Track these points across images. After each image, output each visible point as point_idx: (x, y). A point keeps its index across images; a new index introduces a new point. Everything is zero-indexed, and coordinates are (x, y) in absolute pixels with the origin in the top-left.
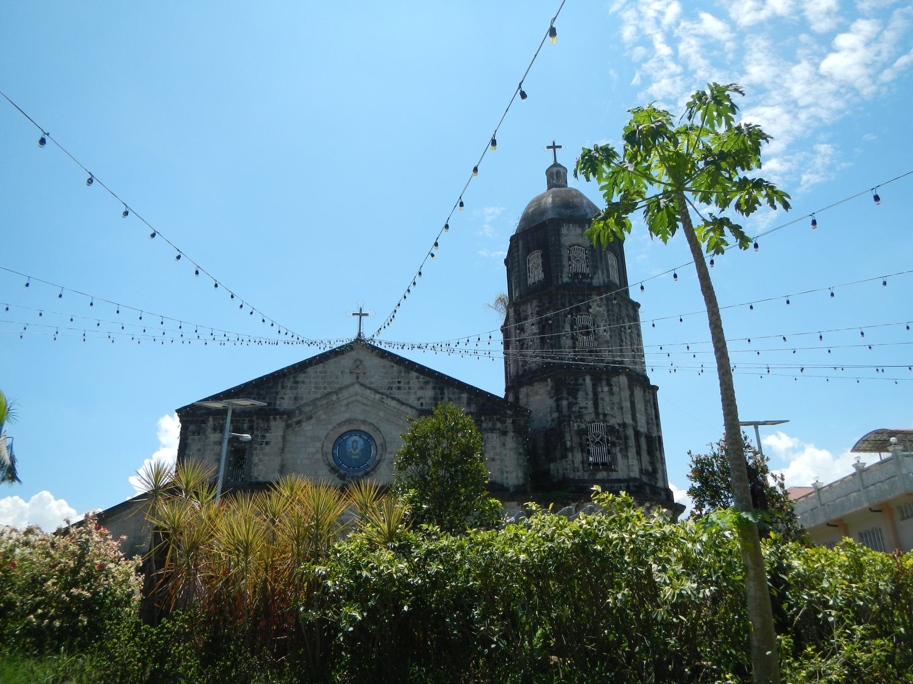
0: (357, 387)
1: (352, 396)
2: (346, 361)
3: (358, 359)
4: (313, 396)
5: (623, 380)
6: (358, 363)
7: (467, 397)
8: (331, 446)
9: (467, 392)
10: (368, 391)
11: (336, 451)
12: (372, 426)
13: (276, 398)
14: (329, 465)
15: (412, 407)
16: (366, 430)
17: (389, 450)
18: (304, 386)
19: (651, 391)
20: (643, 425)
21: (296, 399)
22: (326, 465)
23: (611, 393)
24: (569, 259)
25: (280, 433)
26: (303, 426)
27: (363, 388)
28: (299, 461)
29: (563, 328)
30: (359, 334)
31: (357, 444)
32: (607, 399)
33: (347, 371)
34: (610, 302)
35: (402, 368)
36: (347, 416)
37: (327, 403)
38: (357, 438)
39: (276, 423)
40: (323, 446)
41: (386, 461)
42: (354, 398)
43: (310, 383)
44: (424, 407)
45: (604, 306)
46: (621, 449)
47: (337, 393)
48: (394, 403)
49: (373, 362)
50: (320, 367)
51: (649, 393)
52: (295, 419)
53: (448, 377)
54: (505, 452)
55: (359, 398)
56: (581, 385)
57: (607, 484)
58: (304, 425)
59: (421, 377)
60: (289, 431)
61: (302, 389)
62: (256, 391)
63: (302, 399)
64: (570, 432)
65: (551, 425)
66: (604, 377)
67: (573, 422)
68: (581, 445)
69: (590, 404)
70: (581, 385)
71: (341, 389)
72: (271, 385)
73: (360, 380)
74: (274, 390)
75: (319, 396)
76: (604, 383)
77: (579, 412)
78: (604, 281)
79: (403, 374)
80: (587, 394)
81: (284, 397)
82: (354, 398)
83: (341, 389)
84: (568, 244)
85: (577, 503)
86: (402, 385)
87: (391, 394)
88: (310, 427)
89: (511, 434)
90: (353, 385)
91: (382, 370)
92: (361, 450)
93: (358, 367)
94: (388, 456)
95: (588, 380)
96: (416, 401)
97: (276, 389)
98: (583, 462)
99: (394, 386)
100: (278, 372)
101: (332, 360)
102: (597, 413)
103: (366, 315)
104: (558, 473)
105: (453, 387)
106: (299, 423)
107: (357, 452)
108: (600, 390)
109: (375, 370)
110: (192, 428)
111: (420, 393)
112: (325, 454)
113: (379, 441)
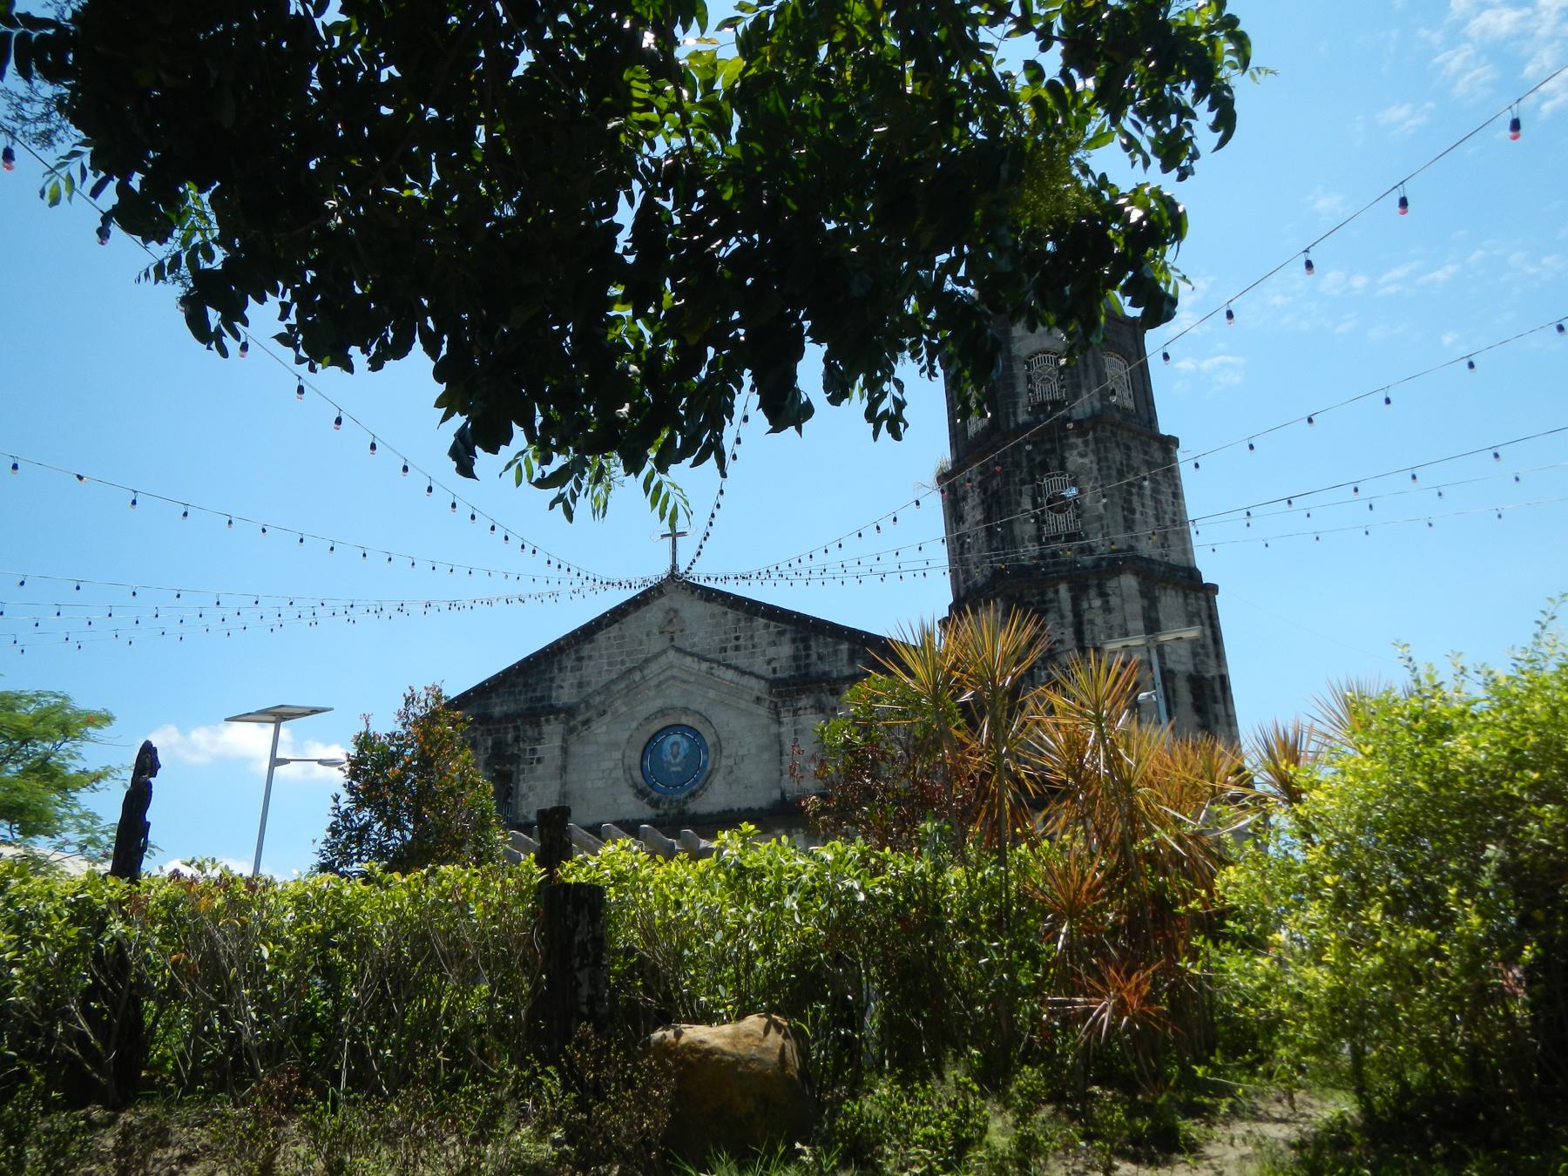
0: (672, 654)
1: (663, 671)
2: (653, 614)
3: (671, 609)
4: (605, 678)
5: (1129, 582)
6: (672, 615)
8: (638, 755)
10: (689, 659)
11: (647, 763)
12: (698, 716)
13: (550, 688)
14: (635, 785)
15: (758, 677)
16: (690, 724)
17: (725, 752)
18: (592, 663)
19: (1201, 595)
20: (1184, 660)
21: (580, 685)
23: (1107, 608)
24: (1029, 380)
25: (557, 742)
27: (681, 655)
28: (589, 785)
29: (1019, 504)
30: (674, 567)
32: (1099, 620)
33: (655, 630)
34: (1101, 445)
35: (741, 615)
38: (677, 738)
42: (668, 673)
43: (601, 657)
44: (779, 675)
45: (1091, 455)
47: (640, 668)
48: (730, 675)
49: (693, 610)
50: (614, 630)
51: (1197, 598)
52: (580, 718)
53: (814, 618)
55: (675, 672)
56: (1051, 601)
58: (594, 726)
59: (772, 624)
60: (573, 738)
61: (589, 669)
62: (521, 680)
63: (589, 683)
66: (1093, 582)
69: (1069, 633)
70: (1051, 601)
71: (647, 661)
72: (543, 667)
73: (676, 643)
74: (548, 676)
75: (614, 676)
76: (1093, 592)
78: (1093, 407)
79: (742, 624)
80: (1062, 617)
82: (668, 673)
83: (647, 661)
84: (1024, 353)
86: (741, 642)
88: (604, 729)
90: (664, 652)
92: (685, 758)
94: (724, 762)
95: (1063, 589)
96: (765, 667)
100: (551, 646)
101: (632, 617)
103: (683, 534)
106: (586, 722)
108: (1085, 605)
109: (700, 624)
111: (771, 652)
112: (628, 770)
113: (709, 739)
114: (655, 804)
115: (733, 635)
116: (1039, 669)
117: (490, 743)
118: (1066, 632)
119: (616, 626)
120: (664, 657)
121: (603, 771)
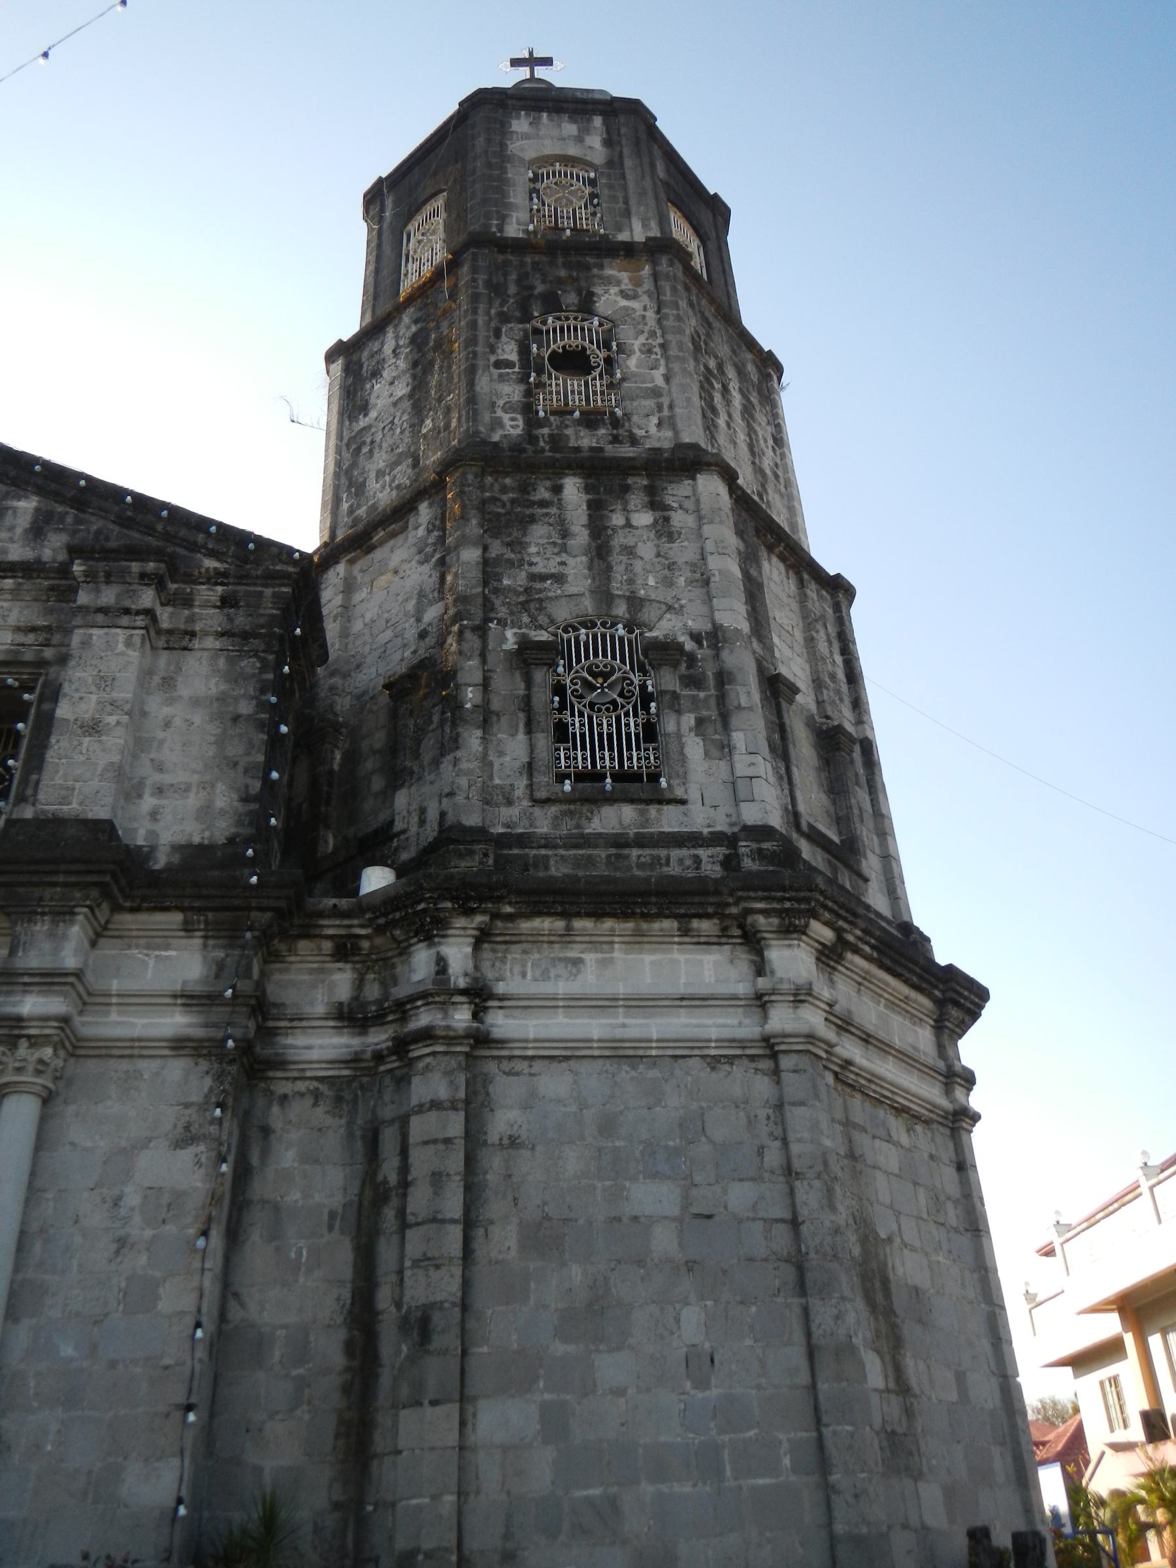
9: (40, 491)
23: (664, 530)
32: (647, 550)
45: (645, 299)
46: (700, 722)
54: (166, 711)
57: (635, 852)
64: (483, 656)
65: (415, 652)
67: (502, 623)
68: (526, 705)
76: (636, 499)
77: (527, 590)
85: (480, 919)
89: (210, 642)
98: (530, 768)
102: (604, 595)
104: (422, 822)
108: (617, 519)
116: (502, 623)
118: (571, 562)
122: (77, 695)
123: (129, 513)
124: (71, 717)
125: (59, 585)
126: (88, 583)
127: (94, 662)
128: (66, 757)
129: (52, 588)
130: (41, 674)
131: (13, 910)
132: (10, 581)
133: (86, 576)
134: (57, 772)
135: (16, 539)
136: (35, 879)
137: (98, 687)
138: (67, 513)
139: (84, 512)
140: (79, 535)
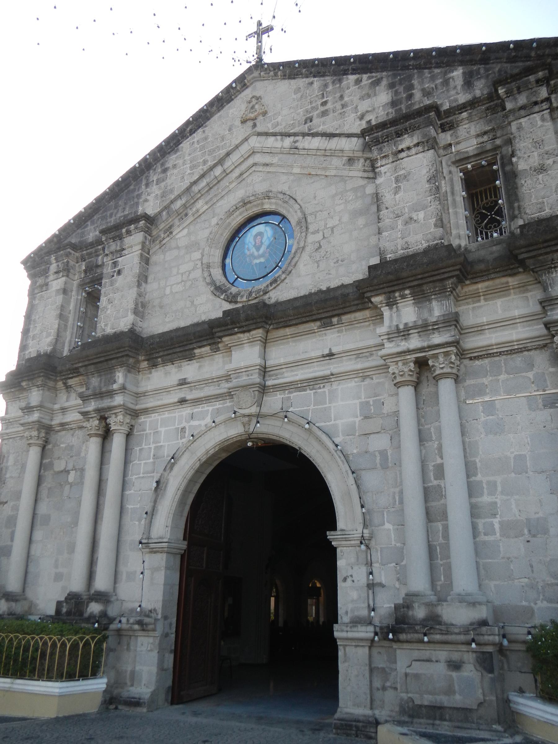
0: (255, 142)
7: (464, 73)
8: (218, 254)
9: (462, 63)
14: (213, 283)
15: (349, 136)
17: (312, 228)
18: (175, 171)
22: (208, 284)
26: (174, 233)
27: (264, 138)
31: (262, 238)
36: (240, 194)
37: (208, 184)
38: (261, 228)
39: (132, 237)
40: (203, 256)
41: (309, 249)
42: (250, 161)
43: (184, 164)
47: (221, 162)
48: (316, 143)
50: (198, 135)
55: (258, 158)
59: (365, 77)
72: (132, 187)
74: (136, 193)
75: (195, 177)
79: (330, 88)
81: (148, 198)
82: (250, 161)
86: (329, 106)
87: (309, 130)
88: (185, 231)
90: (246, 139)
91: (295, 96)
93: (253, 107)
94: (311, 238)
96: (358, 122)
97: (138, 190)
99: (315, 113)
105: (430, 68)
107: (261, 251)
110: (40, 281)
111: (364, 106)
114: (232, 299)
115: (319, 103)
117: (84, 268)
119: (200, 130)
120: (246, 143)
121: (182, 274)
122: (526, 156)
123: (513, 54)
124: (528, 168)
125: (490, 106)
126: (509, 97)
127: (528, 136)
128: (533, 188)
129: (487, 109)
130: (497, 154)
131: (538, 269)
132: (465, 113)
133: (507, 94)
134: (531, 197)
135: (459, 92)
136: (548, 250)
137: (536, 148)
138: (479, 68)
139: (488, 64)
140: (491, 76)
